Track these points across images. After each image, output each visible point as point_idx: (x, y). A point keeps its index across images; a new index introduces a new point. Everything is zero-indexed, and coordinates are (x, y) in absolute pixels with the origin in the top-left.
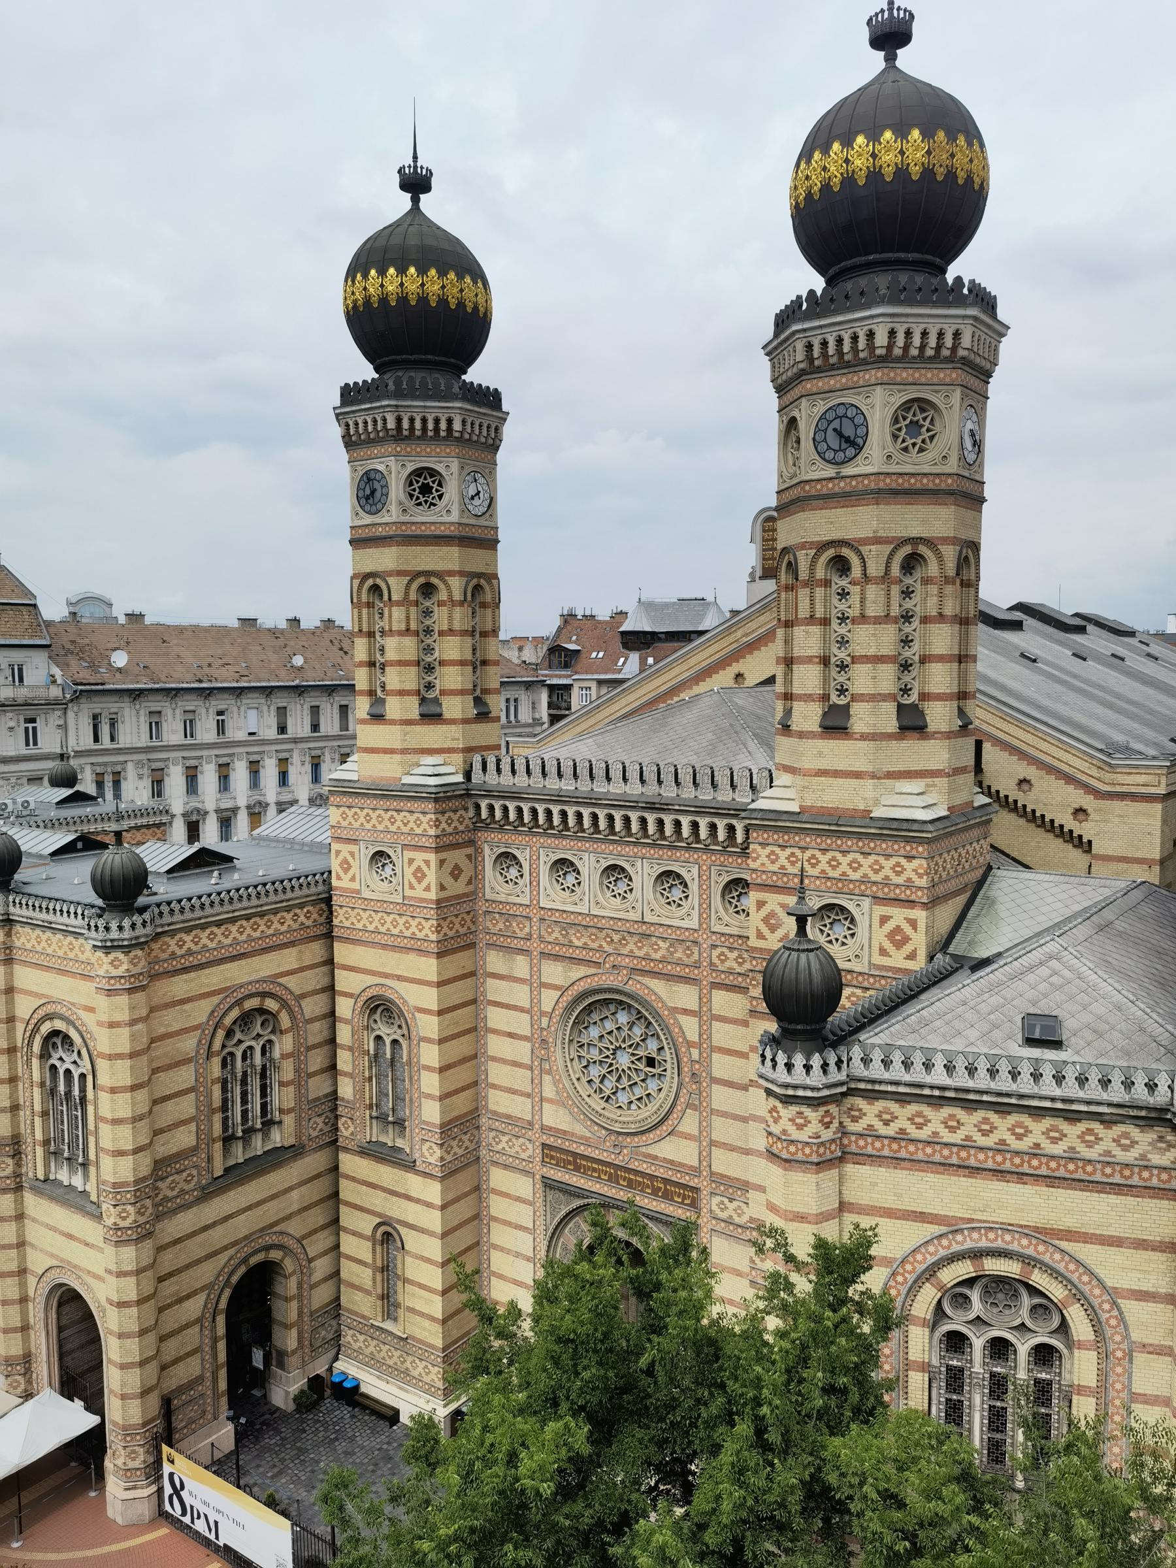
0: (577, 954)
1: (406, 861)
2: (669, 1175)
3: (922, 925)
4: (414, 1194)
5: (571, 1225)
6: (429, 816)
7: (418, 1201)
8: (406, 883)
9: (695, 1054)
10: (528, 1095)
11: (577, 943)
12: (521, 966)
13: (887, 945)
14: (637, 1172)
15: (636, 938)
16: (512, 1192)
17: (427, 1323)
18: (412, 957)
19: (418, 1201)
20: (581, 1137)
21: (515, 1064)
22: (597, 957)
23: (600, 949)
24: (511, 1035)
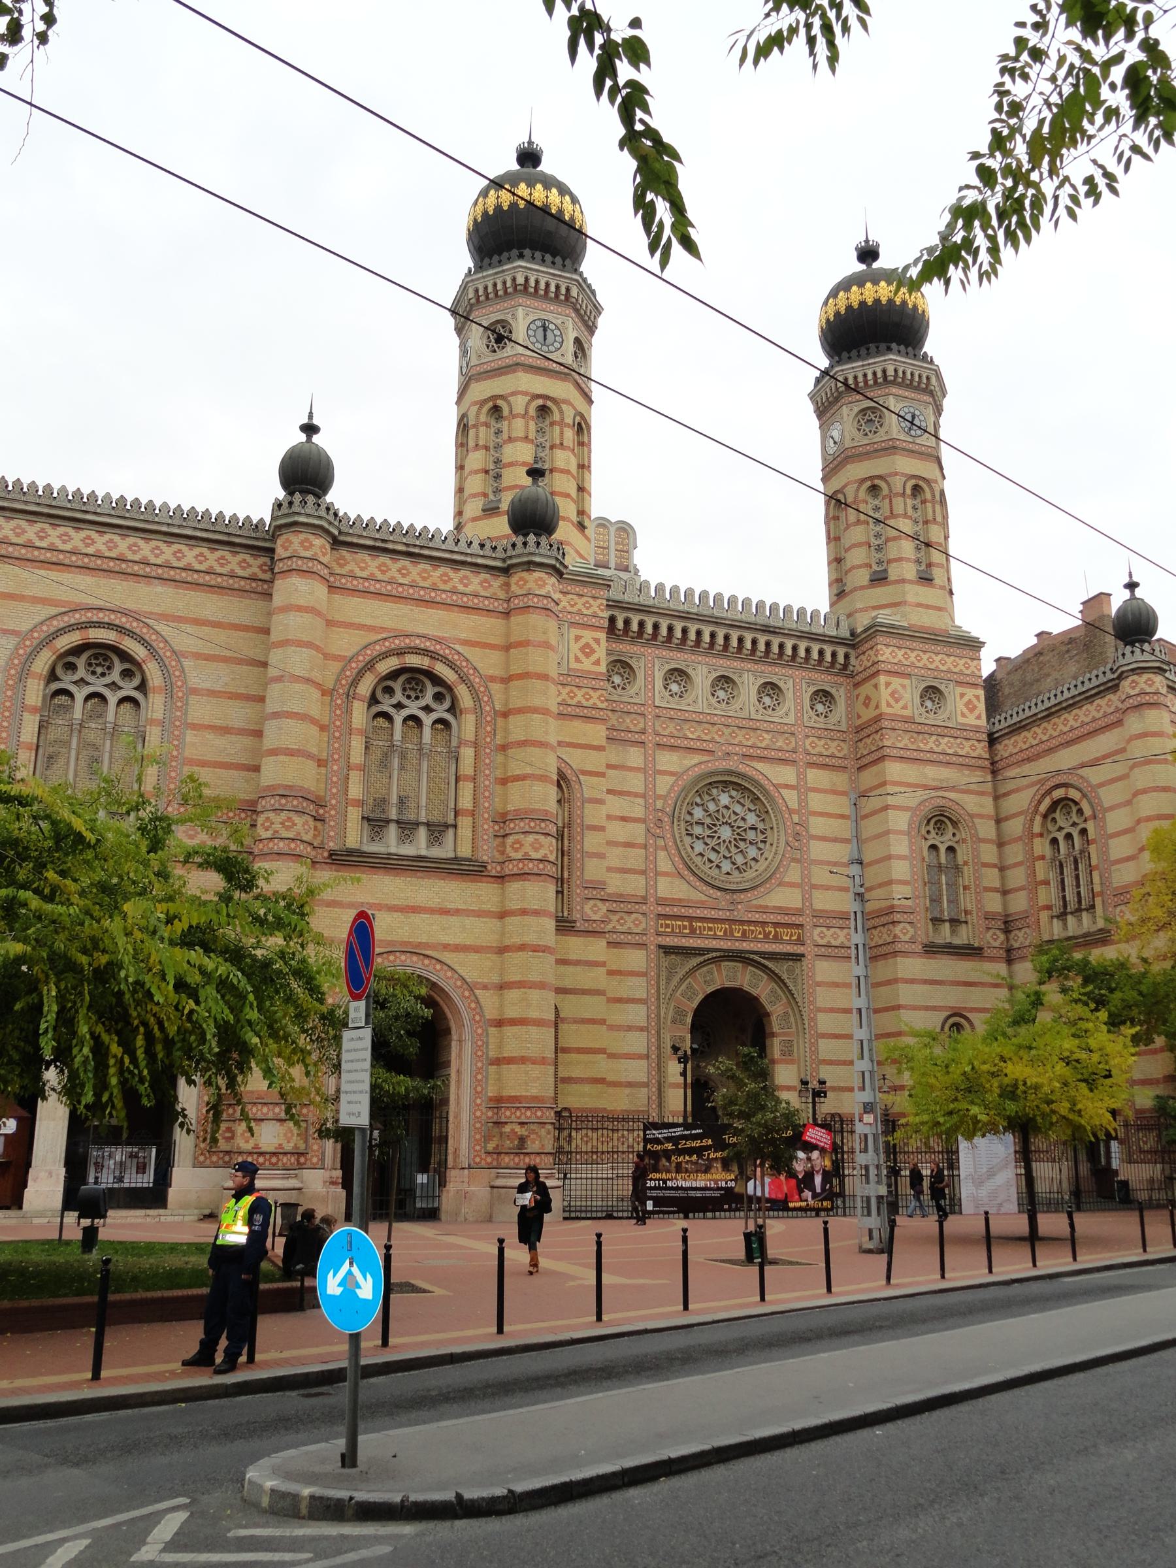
1: (572, 636)
2: (779, 919)
3: (982, 698)
4: (573, 957)
5: (683, 987)
6: (599, 601)
7: (577, 963)
8: (572, 656)
10: (643, 872)
11: (691, 736)
12: (635, 757)
13: (965, 711)
14: (750, 922)
16: (624, 967)
17: (586, 1088)
18: (576, 723)
19: (577, 963)
20: (697, 902)
21: (628, 845)
22: (711, 746)
23: (712, 741)
24: (623, 819)
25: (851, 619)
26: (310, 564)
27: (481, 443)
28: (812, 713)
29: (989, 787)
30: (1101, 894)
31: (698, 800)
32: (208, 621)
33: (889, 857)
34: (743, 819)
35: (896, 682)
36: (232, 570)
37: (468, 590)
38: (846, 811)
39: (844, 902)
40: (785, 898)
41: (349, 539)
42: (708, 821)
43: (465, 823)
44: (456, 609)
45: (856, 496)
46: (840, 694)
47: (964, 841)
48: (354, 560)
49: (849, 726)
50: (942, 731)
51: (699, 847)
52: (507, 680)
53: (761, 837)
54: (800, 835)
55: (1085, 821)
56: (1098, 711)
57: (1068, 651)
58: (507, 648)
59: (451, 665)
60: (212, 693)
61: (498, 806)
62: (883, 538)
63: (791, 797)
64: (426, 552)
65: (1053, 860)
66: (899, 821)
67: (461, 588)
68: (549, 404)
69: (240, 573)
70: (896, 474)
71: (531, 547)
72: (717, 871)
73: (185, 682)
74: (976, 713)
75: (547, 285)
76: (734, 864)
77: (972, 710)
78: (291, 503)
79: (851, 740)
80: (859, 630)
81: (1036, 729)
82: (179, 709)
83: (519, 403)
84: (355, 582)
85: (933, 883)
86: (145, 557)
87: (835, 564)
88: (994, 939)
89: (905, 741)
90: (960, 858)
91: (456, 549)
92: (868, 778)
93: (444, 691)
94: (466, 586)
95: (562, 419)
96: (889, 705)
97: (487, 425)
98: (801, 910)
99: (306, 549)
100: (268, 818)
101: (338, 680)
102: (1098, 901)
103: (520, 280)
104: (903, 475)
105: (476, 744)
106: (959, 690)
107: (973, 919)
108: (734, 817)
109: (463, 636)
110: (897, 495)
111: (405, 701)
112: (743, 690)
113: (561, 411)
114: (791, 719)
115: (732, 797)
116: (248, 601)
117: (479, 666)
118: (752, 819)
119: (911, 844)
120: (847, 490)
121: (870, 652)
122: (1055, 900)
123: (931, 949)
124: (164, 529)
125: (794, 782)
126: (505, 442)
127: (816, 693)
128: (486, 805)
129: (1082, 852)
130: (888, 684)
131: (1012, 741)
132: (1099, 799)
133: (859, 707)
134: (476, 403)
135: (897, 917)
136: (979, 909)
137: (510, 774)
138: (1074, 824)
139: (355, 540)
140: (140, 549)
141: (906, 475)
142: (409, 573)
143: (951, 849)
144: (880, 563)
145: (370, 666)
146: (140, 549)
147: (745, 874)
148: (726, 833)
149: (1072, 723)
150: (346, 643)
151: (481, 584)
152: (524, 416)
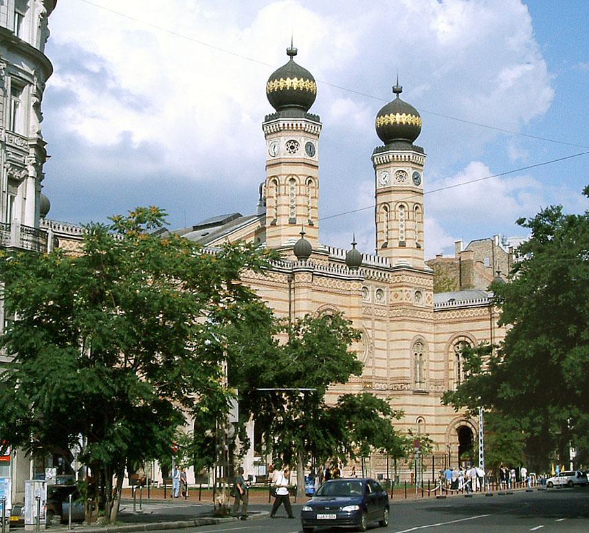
27: (287, 193)
50: (421, 309)
62: (404, 227)
66: (408, 345)
77: (429, 300)
83: (303, 179)
90: (424, 358)
92: (394, 326)
97: (288, 185)
103: (303, 126)
104: (413, 202)
114: (370, 302)
120: (390, 204)
125: (370, 327)
126: (297, 195)
134: (284, 175)
143: (421, 355)
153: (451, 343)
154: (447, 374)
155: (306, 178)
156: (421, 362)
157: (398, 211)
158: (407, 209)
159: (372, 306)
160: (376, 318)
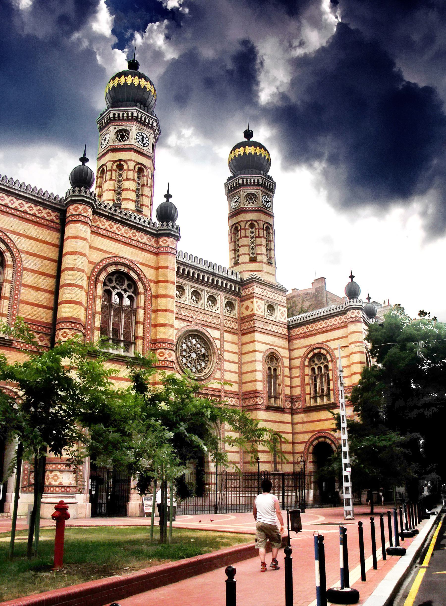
0: (184, 318)
9: (219, 352)
11: (184, 314)
15: (203, 314)
23: (191, 317)
25: (241, 274)
26: (86, 219)
27: (113, 178)
28: (226, 310)
29: (287, 346)
30: (333, 390)
31: (184, 341)
32: (32, 237)
33: (255, 371)
34: (201, 351)
35: (260, 301)
36: (44, 216)
37: (143, 241)
38: (237, 351)
39: (235, 388)
40: (214, 385)
41: (99, 211)
42: (188, 350)
43: (140, 342)
44: (138, 249)
45: (245, 226)
46: (236, 304)
47: (279, 366)
48: (100, 220)
49: (238, 317)
51: (184, 361)
52: (157, 282)
53: (207, 359)
54: (221, 359)
55: (328, 362)
56: (336, 322)
57: (306, 297)
58: (157, 268)
59: (136, 272)
60: (33, 271)
61: (153, 337)
62: (255, 244)
63: (218, 343)
64: (128, 222)
65: (312, 376)
66: (259, 356)
67: (140, 240)
68: (143, 167)
69: (47, 218)
70: (261, 220)
71: (170, 227)
72: (190, 371)
73: (22, 264)
74: (284, 317)
75: (145, 119)
76: (197, 369)
77: (283, 316)
78: (74, 191)
79: (239, 322)
80: (244, 279)
81: (308, 326)
82: (18, 276)
83: (131, 165)
84: (100, 230)
85: (269, 382)
86: (7, 204)
87: (233, 251)
88: (288, 405)
89: (261, 326)
90: (278, 373)
91: (139, 223)
92: (246, 338)
93: (133, 284)
94: (142, 239)
95: (148, 175)
96: (257, 311)
98: (219, 389)
99: (85, 212)
100: (65, 332)
101: (92, 273)
102: (332, 393)
103: (135, 115)
105: (144, 309)
106: (279, 307)
107: (282, 397)
108: (197, 350)
109: (140, 261)
110: (261, 228)
111: (117, 286)
112: (203, 297)
113: (147, 172)
114: (219, 312)
115: (196, 341)
116: (49, 231)
117: (146, 274)
118: (203, 351)
119: (263, 366)
121: (250, 289)
122: (312, 391)
123: (269, 408)
124: (17, 192)
126: (124, 180)
127: (227, 302)
128: (148, 335)
129: (325, 373)
130: (257, 302)
131: (297, 329)
132: (334, 354)
133: (243, 310)
134: (111, 161)
135: (258, 395)
136: (284, 393)
137: (158, 323)
138: (322, 363)
139: (101, 212)
140: (5, 199)
141: (264, 222)
142: (121, 230)
144: (253, 254)
145: (104, 268)
146: (5, 199)
147: (201, 374)
148: (194, 356)
149: (324, 325)
150: (97, 257)
151: (147, 239)
152: (133, 170)
153: (307, 356)
154: (303, 390)
155: (135, 163)
156: (276, 377)
157: (248, 229)
158: (257, 226)
159: (220, 316)
160: (228, 329)
